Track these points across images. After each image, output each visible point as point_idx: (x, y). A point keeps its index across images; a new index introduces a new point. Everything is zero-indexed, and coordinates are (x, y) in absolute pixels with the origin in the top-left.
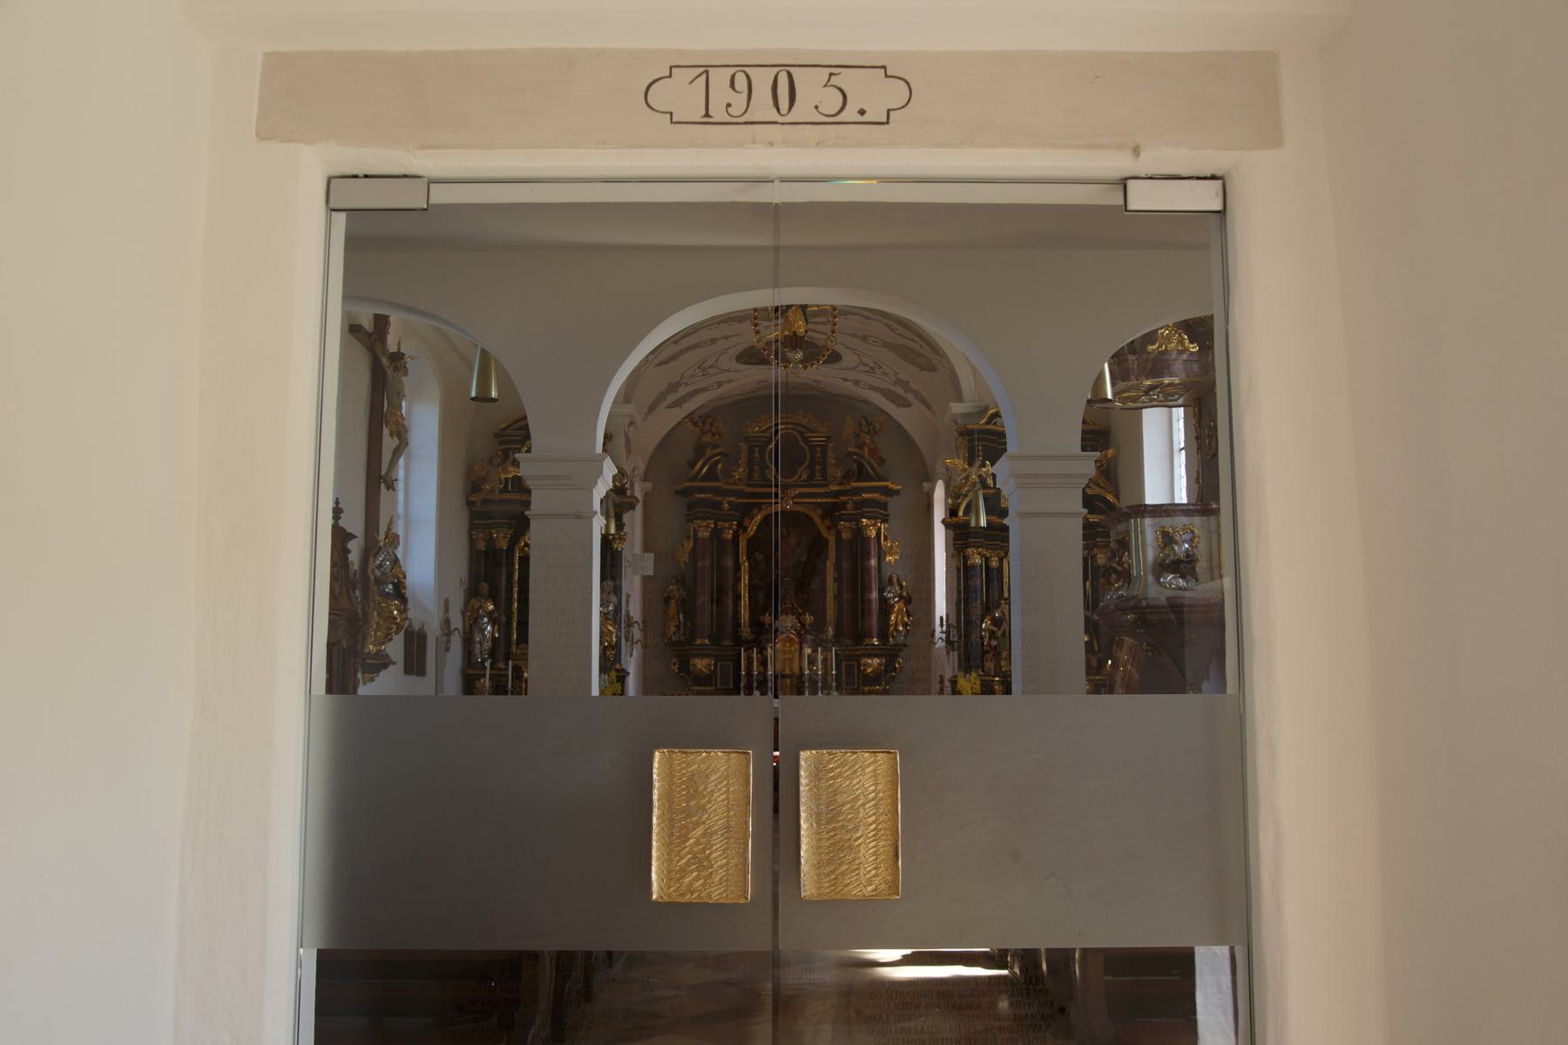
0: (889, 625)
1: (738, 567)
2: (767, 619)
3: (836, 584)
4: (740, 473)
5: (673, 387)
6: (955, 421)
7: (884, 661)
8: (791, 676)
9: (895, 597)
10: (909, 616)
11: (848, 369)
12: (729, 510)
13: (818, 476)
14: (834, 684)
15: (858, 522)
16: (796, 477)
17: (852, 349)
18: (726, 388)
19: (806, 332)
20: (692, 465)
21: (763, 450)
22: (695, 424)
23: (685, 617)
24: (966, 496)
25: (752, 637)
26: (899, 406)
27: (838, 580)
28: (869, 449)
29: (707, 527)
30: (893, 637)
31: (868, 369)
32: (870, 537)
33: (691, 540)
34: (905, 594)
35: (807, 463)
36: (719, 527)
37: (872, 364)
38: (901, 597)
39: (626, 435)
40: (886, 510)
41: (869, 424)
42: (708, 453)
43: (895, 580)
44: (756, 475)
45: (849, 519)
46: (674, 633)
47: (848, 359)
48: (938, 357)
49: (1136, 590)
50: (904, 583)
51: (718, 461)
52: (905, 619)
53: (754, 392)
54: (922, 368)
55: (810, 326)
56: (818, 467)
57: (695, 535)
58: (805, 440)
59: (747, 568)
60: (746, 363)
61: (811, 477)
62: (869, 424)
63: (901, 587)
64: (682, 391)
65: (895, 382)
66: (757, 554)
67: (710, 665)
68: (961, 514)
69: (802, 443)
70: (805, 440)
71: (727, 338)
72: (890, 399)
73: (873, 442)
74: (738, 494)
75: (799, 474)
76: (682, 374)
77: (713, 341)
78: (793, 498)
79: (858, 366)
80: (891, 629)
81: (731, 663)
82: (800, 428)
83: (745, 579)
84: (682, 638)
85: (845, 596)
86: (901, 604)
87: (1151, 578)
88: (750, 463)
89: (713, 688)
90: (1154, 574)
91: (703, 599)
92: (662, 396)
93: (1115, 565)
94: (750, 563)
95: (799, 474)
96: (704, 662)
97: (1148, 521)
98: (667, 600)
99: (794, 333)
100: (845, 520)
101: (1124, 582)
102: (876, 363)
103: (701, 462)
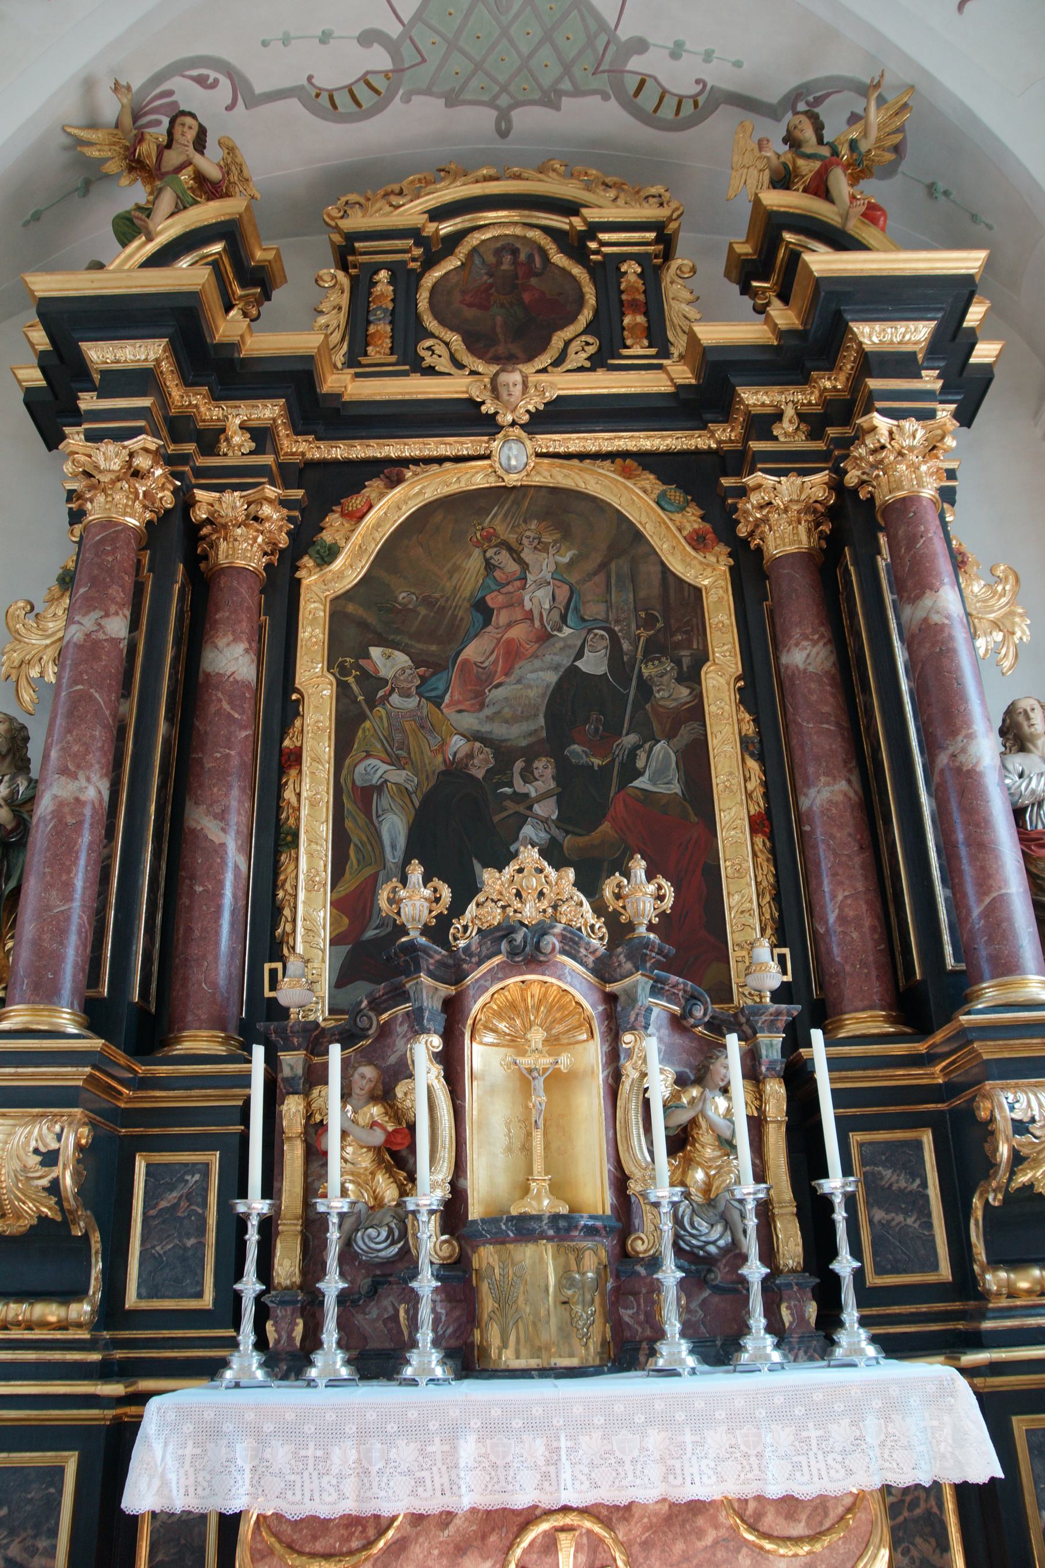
3: (753, 765)
16: (544, 360)
32: (907, 503)
44: (378, 352)
66: (375, 652)
67: (50, 1158)
69: (559, 259)
81: (214, 1158)
89: (82, 1310)
94: (342, 689)
95: (558, 340)
96: (21, 1132)
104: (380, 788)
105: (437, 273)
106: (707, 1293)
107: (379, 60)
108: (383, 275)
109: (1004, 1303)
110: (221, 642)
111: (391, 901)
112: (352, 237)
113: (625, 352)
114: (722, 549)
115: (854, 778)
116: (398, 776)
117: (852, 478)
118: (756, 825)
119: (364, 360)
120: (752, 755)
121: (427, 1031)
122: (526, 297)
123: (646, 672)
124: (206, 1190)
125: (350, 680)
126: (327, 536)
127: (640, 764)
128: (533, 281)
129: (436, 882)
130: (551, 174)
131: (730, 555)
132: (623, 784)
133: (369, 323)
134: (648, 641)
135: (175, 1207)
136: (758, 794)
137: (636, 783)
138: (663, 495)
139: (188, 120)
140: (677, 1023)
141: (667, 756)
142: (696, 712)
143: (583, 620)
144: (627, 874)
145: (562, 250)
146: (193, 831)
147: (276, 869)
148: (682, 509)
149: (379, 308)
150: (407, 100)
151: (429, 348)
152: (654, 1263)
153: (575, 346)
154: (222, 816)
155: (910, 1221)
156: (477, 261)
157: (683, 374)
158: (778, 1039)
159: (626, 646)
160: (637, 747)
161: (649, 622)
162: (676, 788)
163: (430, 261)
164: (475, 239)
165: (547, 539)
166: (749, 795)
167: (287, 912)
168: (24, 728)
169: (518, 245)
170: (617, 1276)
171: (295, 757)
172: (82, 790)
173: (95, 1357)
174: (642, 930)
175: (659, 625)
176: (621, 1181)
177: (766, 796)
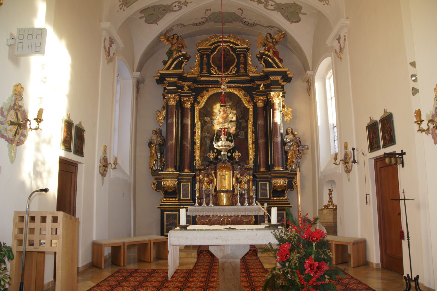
0: (287, 159)
1: (194, 125)
7: (287, 181)
8: (227, 192)
9: (291, 141)
12: (187, 90)
13: (242, 71)
14: (254, 196)
21: (208, 56)
22: (168, 40)
23: (161, 154)
25: (202, 168)
26: (292, 22)
29: (174, 98)
30: (290, 166)
36: (182, 100)
43: (290, 131)
44: (205, 72)
45: (261, 94)
46: (154, 165)
56: (242, 66)
57: (167, 104)
61: (237, 72)
66: (205, 117)
70: (234, 50)
73: (275, 48)
74: (195, 80)
75: (230, 71)
78: (227, 83)
80: (289, 161)
81: (189, 183)
82: (230, 45)
95: (231, 69)
98: (150, 144)
103: (171, 60)
104: (206, 137)
106: (242, 198)
107: (205, 20)
108: (205, 56)
109: (273, 201)
110: (186, 119)
111: (209, 155)
112: (200, 49)
113: (240, 72)
114: (252, 103)
115: (265, 139)
116: (209, 135)
117: (269, 97)
118: (253, 143)
119: (203, 73)
120: (254, 134)
121: (213, 170)
122: (226, 60)
123: (241, 121)
124: (189, 187)
125: (202, 121)
126: (198, 100)
127: (239, 134)
128: (228, 57)
129: (214, 153)
130: (231, 37)
131: (253, 104)
132: (237, 137)
133: (203, 65)
134: (241, 116)
135: (185, 189)
136: (254, 139)
137: (239, 137)
138: (245, 94)
139: (176, 36)
140: (241, 169)
141: (243, 133)
142: (247, 127)
143: (233, 113)
144: (235, 153)
146: (184, 145)
147: (194, 147)
148: (247, 96)
149: (205, 63)
150: (208, 23)
151: (212, 69)
152: (237, 195)
153: (233, 69)
154: (188, 143)
155: (265, 192)
156: (219, 52)
157: (248, 78)
158: (252, 172)
159: (238, 117)
160: (239, 132)
161: (242, 114)
162: (244, 137)
164: (218, 48)
165: (228, 100)
166: (253, 139)
167: (195, 153)
168: (161, 130)
169: (225, 49)
170: (232, 196)
171: (195, 132)
172: (173, 142)
173: (179, 204)
174: (237, 159)
175: (243, 114)
176: (233, 187)
177: (255, 139)
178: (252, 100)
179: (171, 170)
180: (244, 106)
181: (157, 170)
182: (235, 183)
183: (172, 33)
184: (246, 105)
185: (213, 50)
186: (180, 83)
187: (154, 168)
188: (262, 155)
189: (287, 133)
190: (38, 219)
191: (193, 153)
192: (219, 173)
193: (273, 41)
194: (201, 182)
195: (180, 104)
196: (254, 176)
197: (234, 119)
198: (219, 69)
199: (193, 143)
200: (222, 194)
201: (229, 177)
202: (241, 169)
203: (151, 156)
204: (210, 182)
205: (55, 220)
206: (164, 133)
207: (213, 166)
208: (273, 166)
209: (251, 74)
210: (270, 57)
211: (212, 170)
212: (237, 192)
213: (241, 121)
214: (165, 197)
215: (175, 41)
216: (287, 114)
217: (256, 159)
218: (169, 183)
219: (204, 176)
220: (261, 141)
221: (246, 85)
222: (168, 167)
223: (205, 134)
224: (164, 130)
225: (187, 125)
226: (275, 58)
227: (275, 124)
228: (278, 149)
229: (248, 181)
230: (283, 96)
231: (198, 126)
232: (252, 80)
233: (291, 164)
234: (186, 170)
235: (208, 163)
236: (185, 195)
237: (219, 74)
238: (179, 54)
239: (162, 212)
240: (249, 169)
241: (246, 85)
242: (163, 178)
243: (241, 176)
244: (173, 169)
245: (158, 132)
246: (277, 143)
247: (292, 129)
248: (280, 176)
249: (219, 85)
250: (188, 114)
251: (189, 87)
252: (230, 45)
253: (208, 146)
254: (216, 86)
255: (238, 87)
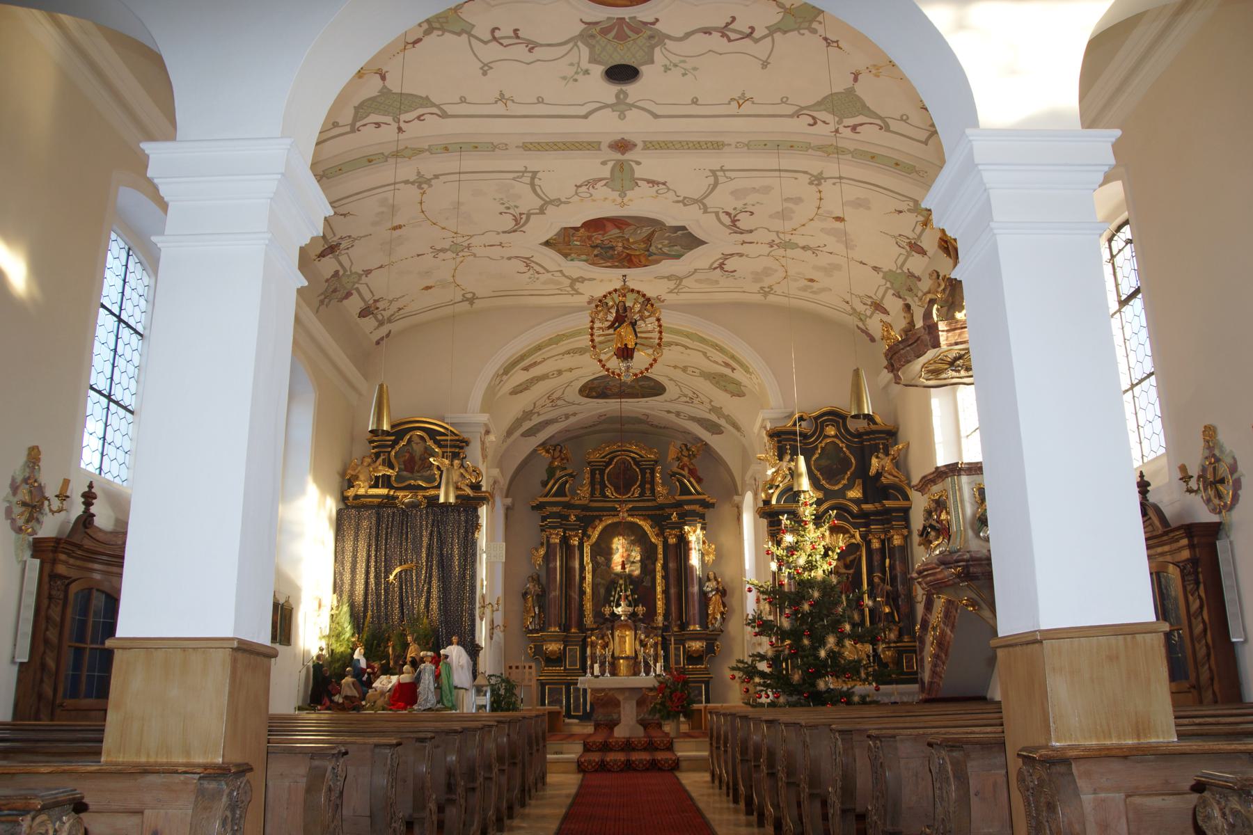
0: (707, 614)
2: (607, 610)
4: (584, 492)
5: (527, 415)
6: (765, 428)
8: (627, 658)
9: (711, 591)
10: (724, 606)
11: (671, 401)
13: (648, 493)
15: (682, 529)
17: (674, 381)
18: (572, 420)
19: (636, 344)
20: (545, 484)
21: (602, 472)
22: (547, 451)
24: (778, 486)
25: (594, 626)
26: (713, 433)
27: (665, 577)
28: (690, 470)
31: (688, 399)
33: (545, 546)
34: (721, 588)
35: (638, 484)
37: (691, 394)
38: (717, 590)
39: (483, 443)
40: (704, 520)
41: (688, 450)
42: (558, 474)
43: (711, 576)
47: (672, 391)
48: (748, 376)
49: (956, 544)
50: (719, 580)
51: (566, 482)
52: (722, 608)
53: (594, 425)
54: (733, 395)
55: (638, 341)
56: (648, 486)
57: (548, 541)
58: (637, 463)
59: (591, 569)
60: (587, 396)
61: (642, 494)
62: (688, 450)
63: (718, 583)
64: (536, 420)
65: (710, 410)
66: (598, 557)
68: (774, 502)
69: (634, 467)
70: (637, 463)
71: (571, 370)
72: (706, 428)
73: (692, 464)
74: (585, 508)
76: (535, 404)
77: (560, 372)
79: (679, 397)
80: (710, 617)
82: (632, 455)
83: (589, 577)
84: (538, 627)
85: (673, 591)
86: (718, 597)
87: (970, 533)
88: (592, 484)
90: (973, 529)
91: (555, 593)
92: (518, 422)
93: (934, 523)
97: (964, 479)
98: (525, 595)
99: (626, 345)
100: (673, 528)
101: (944, 538)
102: (694, 393)
105: (607, 472)
116: (603, 582)
140: (646, 628)
145: (635, 464)
162: (650, 585)
163: (607, 466)
176: (636, 651)
178: (661, 533)
179: (554, 629)
180: (651, 541)
181: (535, 629)
182: (638, 647)
183: (554, 443)
184: (653, 540)
185: (609, 463)
186: (565, 511)
187: (530, 628)
188: (673, 608)
189: (709, 580)
190: (514, 668)
191: (581, 606)
192: (617, 633)
193: (689, 455)
194: (593, 645)
195: (565, 540)
196: (663, 637)
197: (638, 558)
198: (617, 490)
199: (582, 593)
200: (621, 661)
201: (630, 640)
202: (646, 628)
203: (527, 611)
204: (605, 646)
205: (530, 667)
206: (544, 580)
207: (609, 625)
208: (688, 624)
209: (660, 500)
210: (684, 477)
211: (608, 629)
212: (641, 658)
213: (647, 562)
214: (546, 666)
215: (557, 454)
216: (708, 554)
217: (667, 615)
218: (553, 647)
219: (597, 638)
220: (673, 591)
221: (653, 512)
222: (550, 625)
223: (599, 580)
224: (543, 574)
225: (574, 569)
226: (692, 479)
227: (692, 567)
228: (694, 601)
229: (656, 644)
230: (702, 529)
231: (589, 568)
232: (661, 507)
233: (713, 621)
234: (573, 630)
235: (602, 621)
236: (573, 663)
237: (616, 497)
238: (563, 473)
239: (543, 685)
240: (656, 628)
241: (653, 512)
242: (545, 641)
243: (646, 637)
244: (557, 629)
245: (536, 579)
246: (693, 594)
247: (715, 574)
248: (696, 637)
249: (616, 513)
250: (574, 557)
251: (575, 516)
252: (632, 455)
253: (602, 596)
254: (613, 513)
255: (642, 515)
